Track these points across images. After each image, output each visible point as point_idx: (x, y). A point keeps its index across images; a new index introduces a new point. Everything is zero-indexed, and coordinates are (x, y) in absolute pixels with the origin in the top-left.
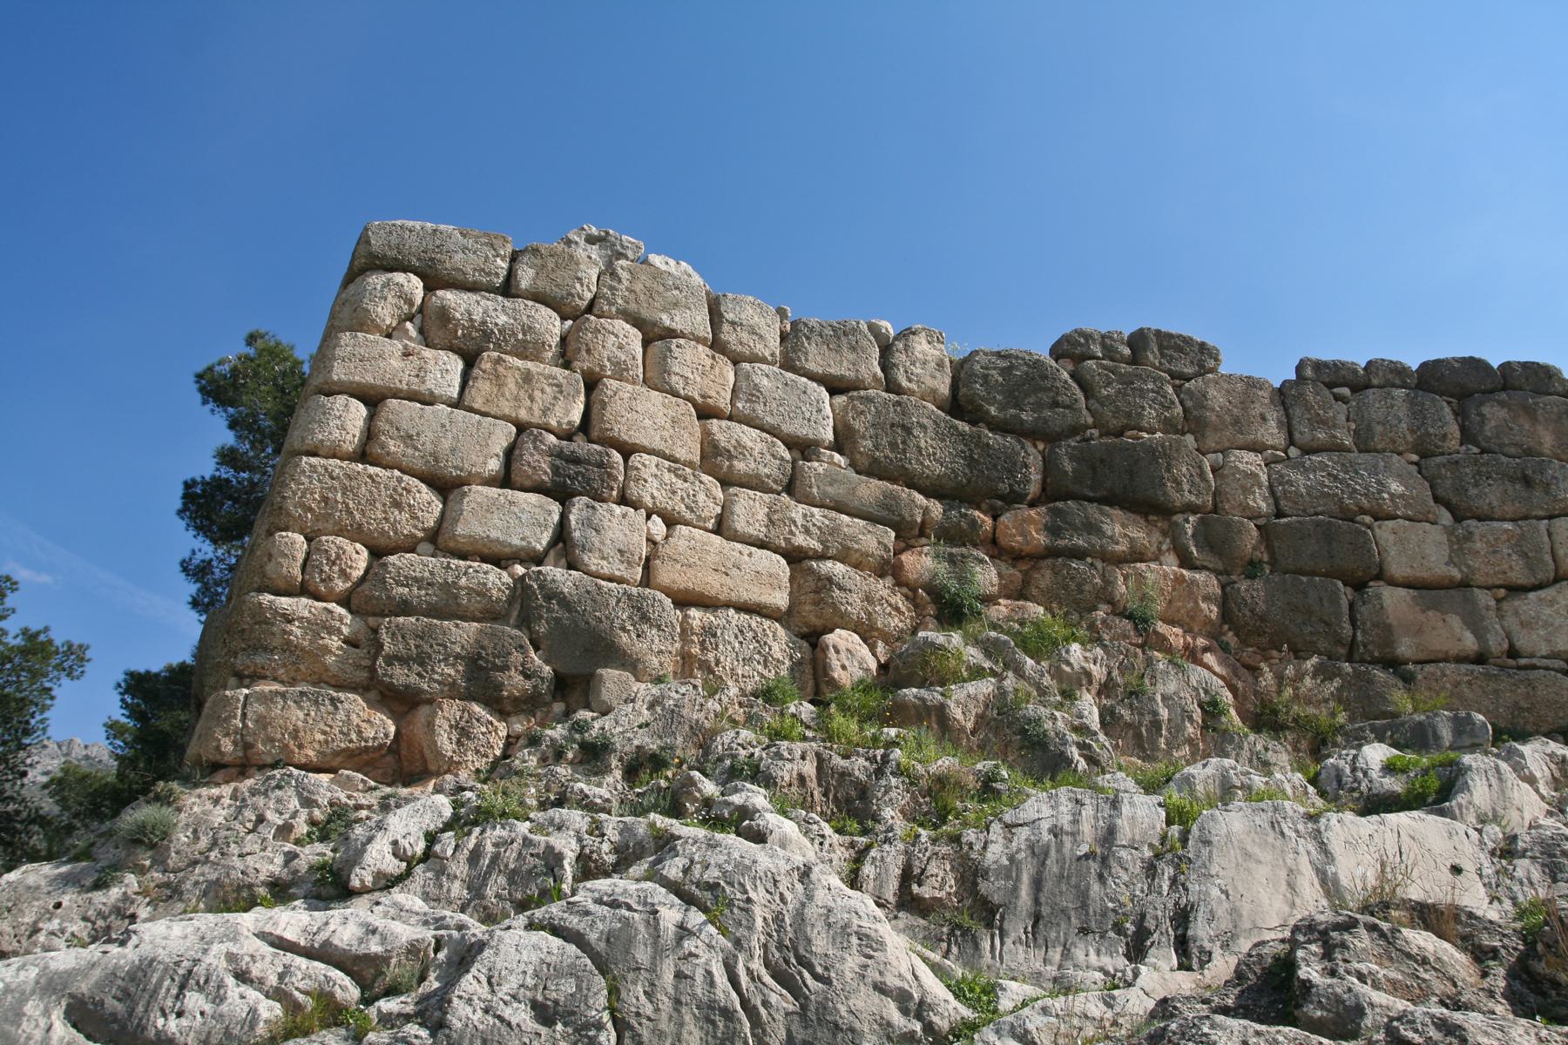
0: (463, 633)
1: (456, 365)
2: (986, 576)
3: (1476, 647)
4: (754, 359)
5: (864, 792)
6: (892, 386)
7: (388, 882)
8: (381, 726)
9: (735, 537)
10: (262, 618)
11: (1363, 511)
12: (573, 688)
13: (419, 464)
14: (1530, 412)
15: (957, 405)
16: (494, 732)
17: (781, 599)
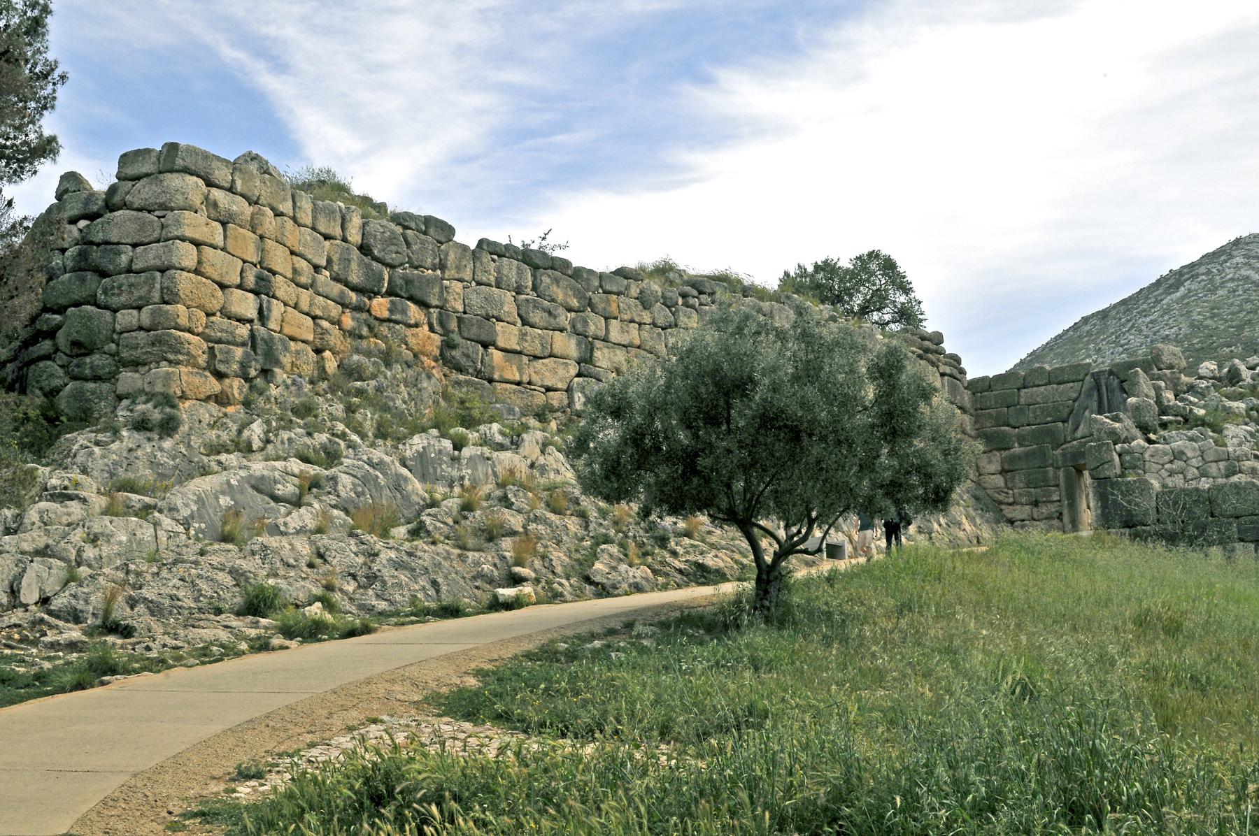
0: (239, 352)
6: (344, 240)
9: (301, 312)
13: (217, 278)
15: (364, 249)
17: (310, 337)
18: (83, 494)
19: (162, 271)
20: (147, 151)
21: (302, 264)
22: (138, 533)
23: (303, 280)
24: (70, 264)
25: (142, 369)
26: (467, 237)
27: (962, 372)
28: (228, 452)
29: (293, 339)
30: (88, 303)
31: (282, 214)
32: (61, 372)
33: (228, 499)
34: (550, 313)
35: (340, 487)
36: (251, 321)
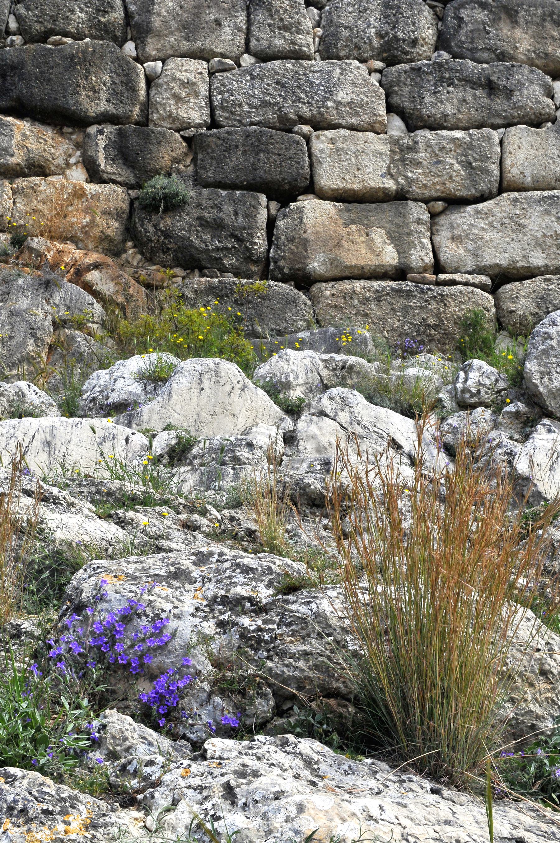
3: (395, 262)
11: (303, 120)
34: (491, 87)
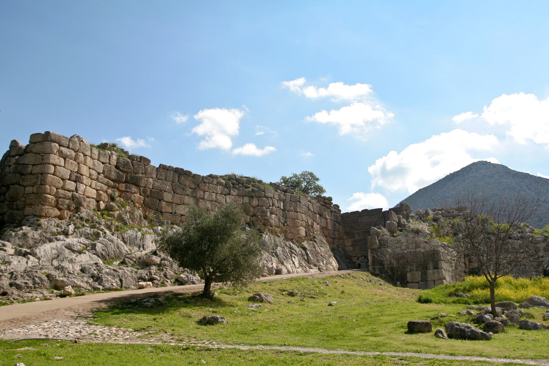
0: (67, 201)
1: (62, 160)
2: (117, 193)
4: (95, 159)
5: (110, 227)
6: (110, 164)
7: (72, 234)
8: (59, 213)
10: (46, 198)
12: (77, 210)
14: (187, 179)
15: (116, 167)
16: (70, 213)
17: (95, 197)
18: (5, 248)
19: (42, 174)
20: (40, 134)
21: (94, 172)
22: (21, 261)
23: (93, 177)
24: (11, 171)
25: (33, 207)
26: (155, 163)
27: (340, 211)
28: (60, 235)
29: (88, 197)
30: (16, 184)
31: (86, 155)
32: (6, 207)
33: (55, 251)
35: (97, 247)
36: (73, 191)
